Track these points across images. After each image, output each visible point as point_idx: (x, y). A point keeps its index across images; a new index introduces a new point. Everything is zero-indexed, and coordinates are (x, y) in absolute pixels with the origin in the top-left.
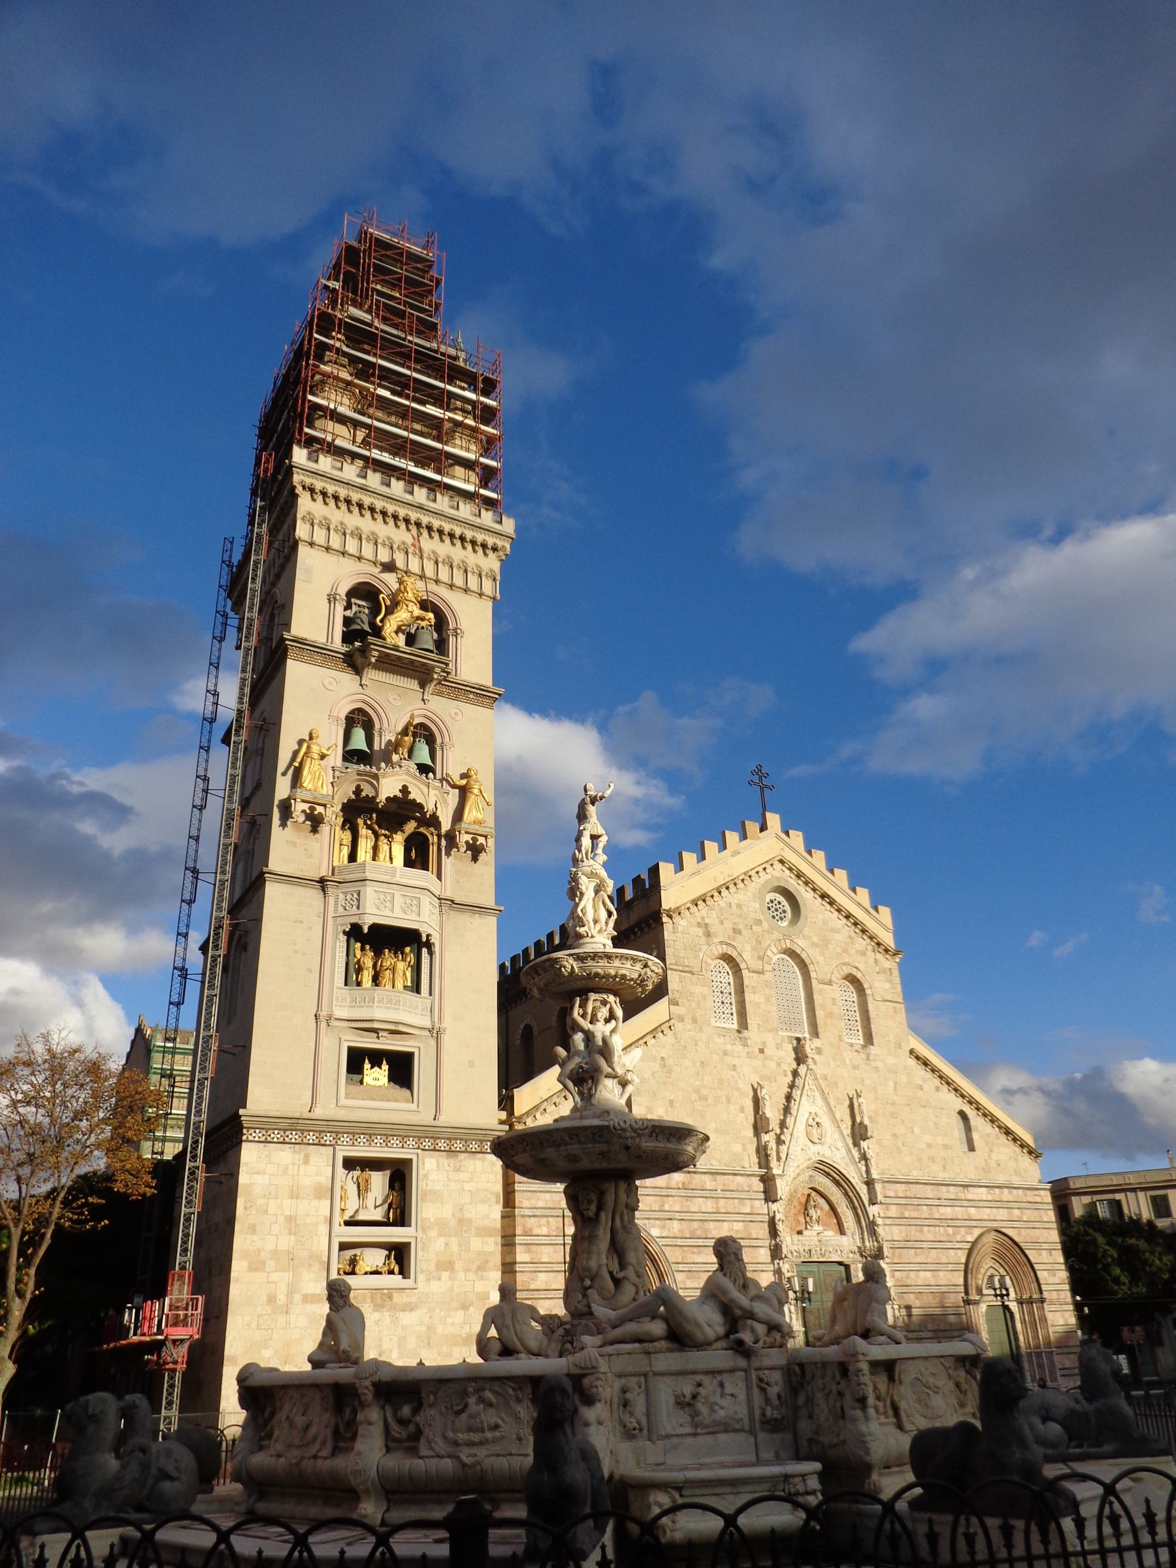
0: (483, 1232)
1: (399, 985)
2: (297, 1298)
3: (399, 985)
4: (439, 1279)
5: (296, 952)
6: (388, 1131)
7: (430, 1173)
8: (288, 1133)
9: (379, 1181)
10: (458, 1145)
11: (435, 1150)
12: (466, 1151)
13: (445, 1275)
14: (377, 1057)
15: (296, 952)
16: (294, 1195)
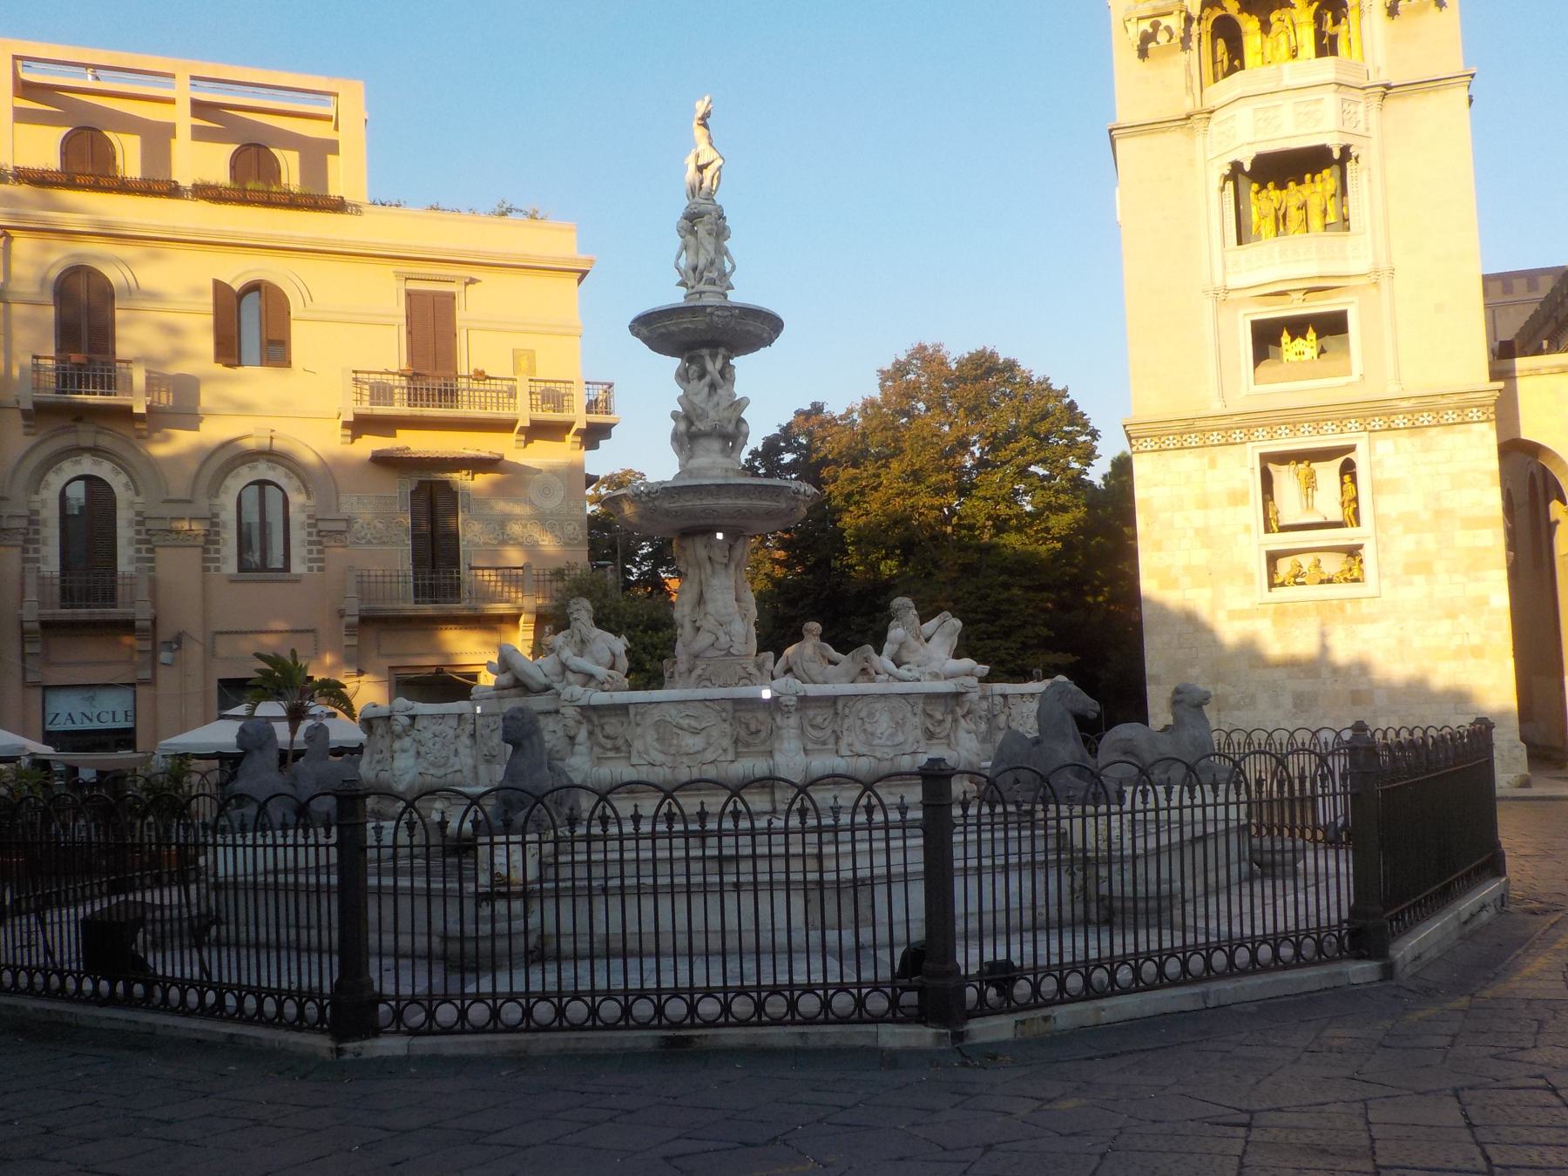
0: (1472, 523)
1: (1316, 222)
3: (1316, 222)
4: (1411, 583)
6: (1317, 416)
7: (1377, 456)
9: (1328, 472)
10: (1426, 418)
11: (1389, 429)
12: (1439, 425)
13: (1419, 579)
14: (1297, 326)
16: (1204, 503)
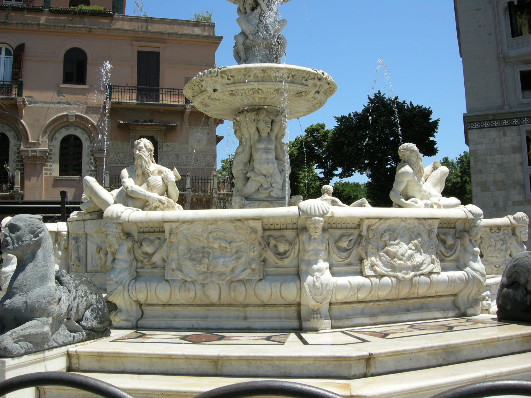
2: (510, 203)
5: (480, 26)
8: (492, 122)
15: (480, 26)
16: (501, 152)
